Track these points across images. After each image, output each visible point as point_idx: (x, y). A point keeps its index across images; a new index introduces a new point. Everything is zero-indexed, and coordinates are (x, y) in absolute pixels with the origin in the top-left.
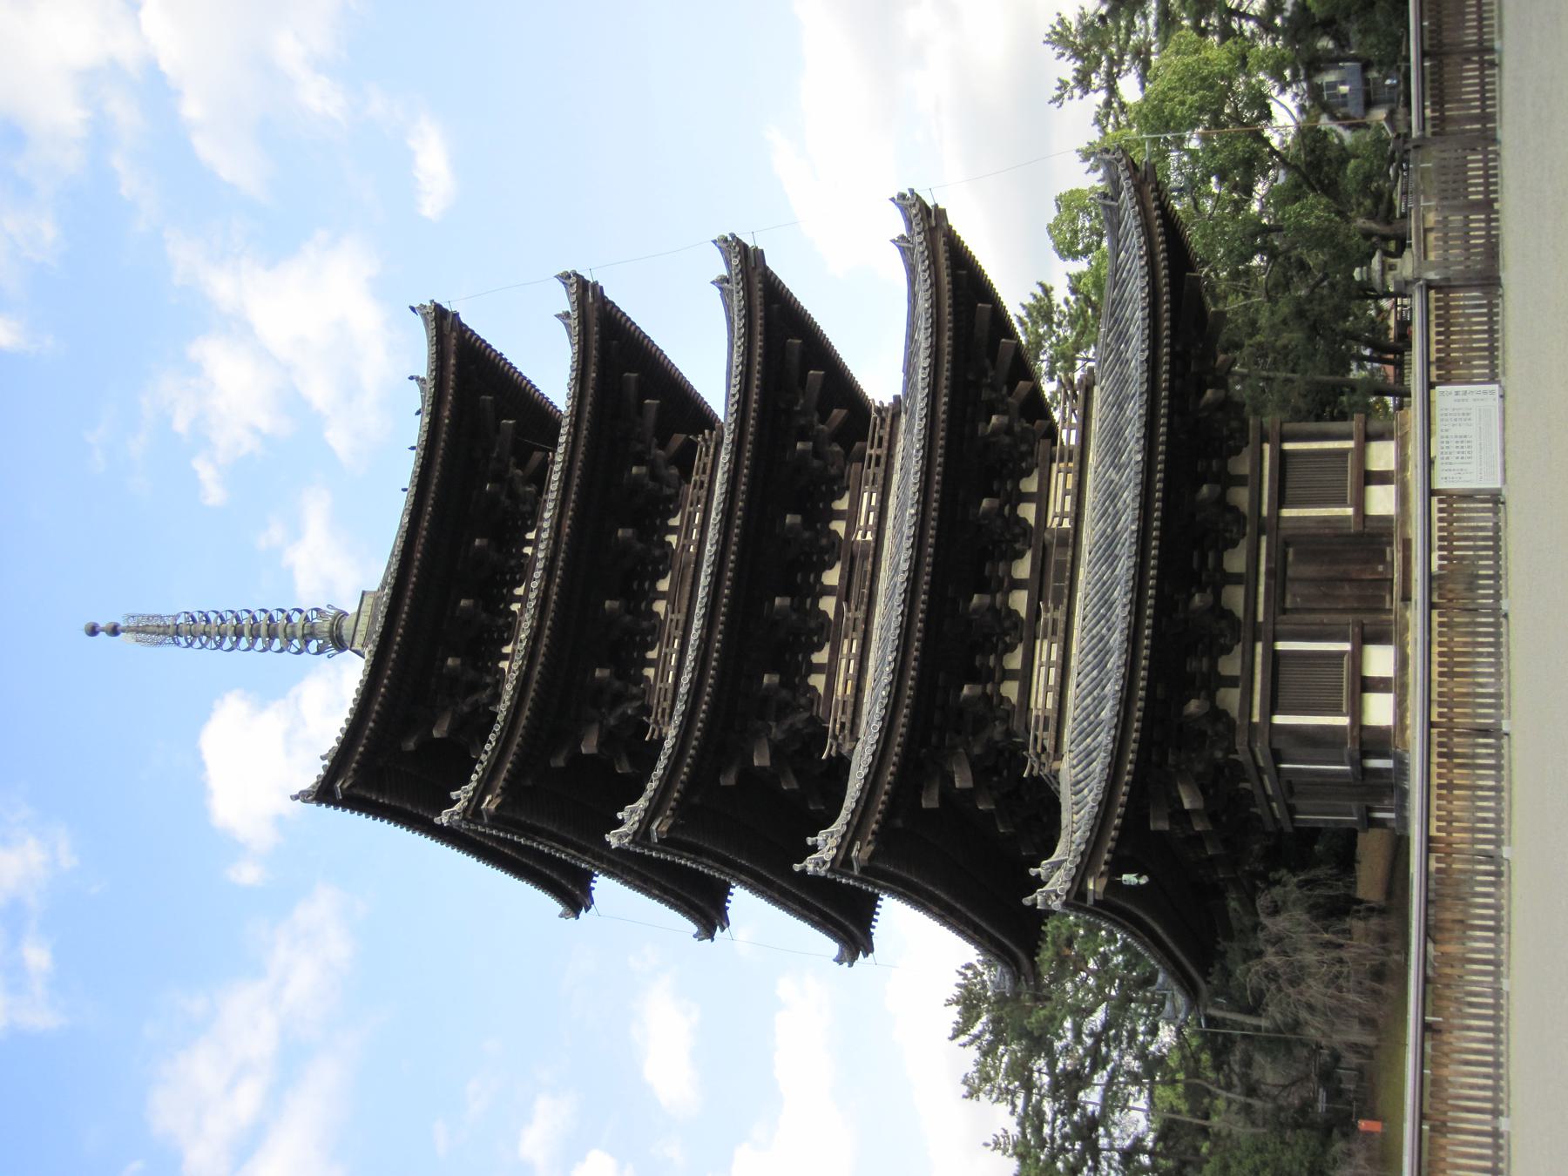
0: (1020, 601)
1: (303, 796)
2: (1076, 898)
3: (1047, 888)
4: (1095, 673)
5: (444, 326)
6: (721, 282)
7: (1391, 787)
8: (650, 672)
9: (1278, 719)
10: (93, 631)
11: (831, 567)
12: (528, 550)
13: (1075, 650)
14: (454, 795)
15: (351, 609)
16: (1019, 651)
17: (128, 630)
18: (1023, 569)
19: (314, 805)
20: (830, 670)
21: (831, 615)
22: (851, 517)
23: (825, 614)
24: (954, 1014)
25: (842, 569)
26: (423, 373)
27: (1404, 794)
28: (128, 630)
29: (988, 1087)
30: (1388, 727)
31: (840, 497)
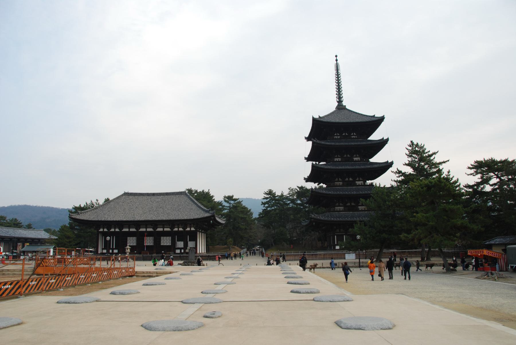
0: (349, 204)
1: (313, 118)
2: (311, 218)
3: (312, 215)
4: (338, 216)
5: (382, 119)
6: (388, 162)
7: (331, 249)
8: (336, 156)
9: (336, 236)
10: (336, 56)
11: (352, 179)
12: (352, 134)
13: (342, 212)
14: (316, 138)
15: (344, 103)
16: (342, 205)
17: (337, 62)
18: (353, 204)
19: (312, 118)
20: (338, 181)
21: (346, 180)
22: (359, 181)
23: (345, 179)
24: (300, 186)
25: (351, 181)
26: (376, 116)
27: (330, 250)
28: (337, 62)
29: (290, 191)
30: (335, 248)
31: (362, 178)
